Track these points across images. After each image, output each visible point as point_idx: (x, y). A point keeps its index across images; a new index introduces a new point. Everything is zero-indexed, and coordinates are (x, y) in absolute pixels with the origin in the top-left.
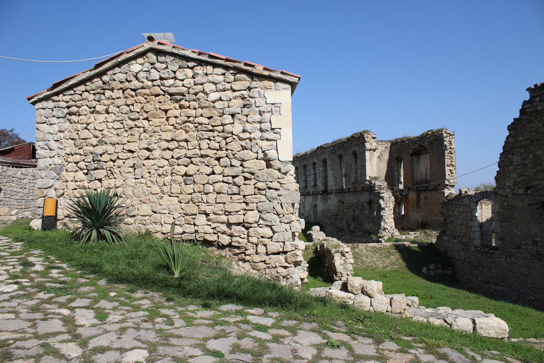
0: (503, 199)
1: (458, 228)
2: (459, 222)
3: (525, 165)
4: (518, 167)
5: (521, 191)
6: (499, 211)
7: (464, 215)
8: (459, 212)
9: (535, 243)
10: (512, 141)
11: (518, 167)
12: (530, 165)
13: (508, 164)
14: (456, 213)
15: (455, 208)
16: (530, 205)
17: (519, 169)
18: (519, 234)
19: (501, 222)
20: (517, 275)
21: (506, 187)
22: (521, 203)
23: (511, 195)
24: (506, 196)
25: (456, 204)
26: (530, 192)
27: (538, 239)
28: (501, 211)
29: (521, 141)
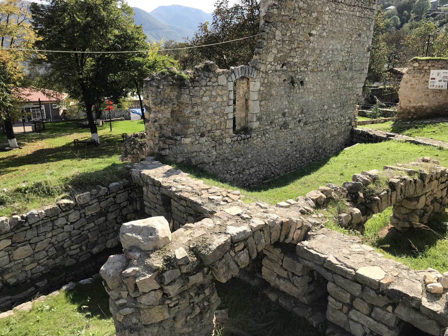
0: (264, 75)
1: (209, 120)
2: (210, 111)
3: (283, 41)
4: (279, 43)
5: (279, 68)
6: (260, 90)
7: (219, 99)
8: (211, 96)
9: (284, 114)
10: (276, 13)
11: (279, 43)
12: (287, 42)
13: (271, 37)
14: (205, 99)
15: (205, 92)
16: (284, 80)
17: (280, 45)
18: (274, 110)
19: (261, 101)
20: (269, 149)
21: (268, 63)
22: (278, 79)
23: (271, 71)
24: (266, 73)
25: (206, 86)
26: (285, 68)
27: (286, 110)
28: (262, 89)
29: (283, 16)
